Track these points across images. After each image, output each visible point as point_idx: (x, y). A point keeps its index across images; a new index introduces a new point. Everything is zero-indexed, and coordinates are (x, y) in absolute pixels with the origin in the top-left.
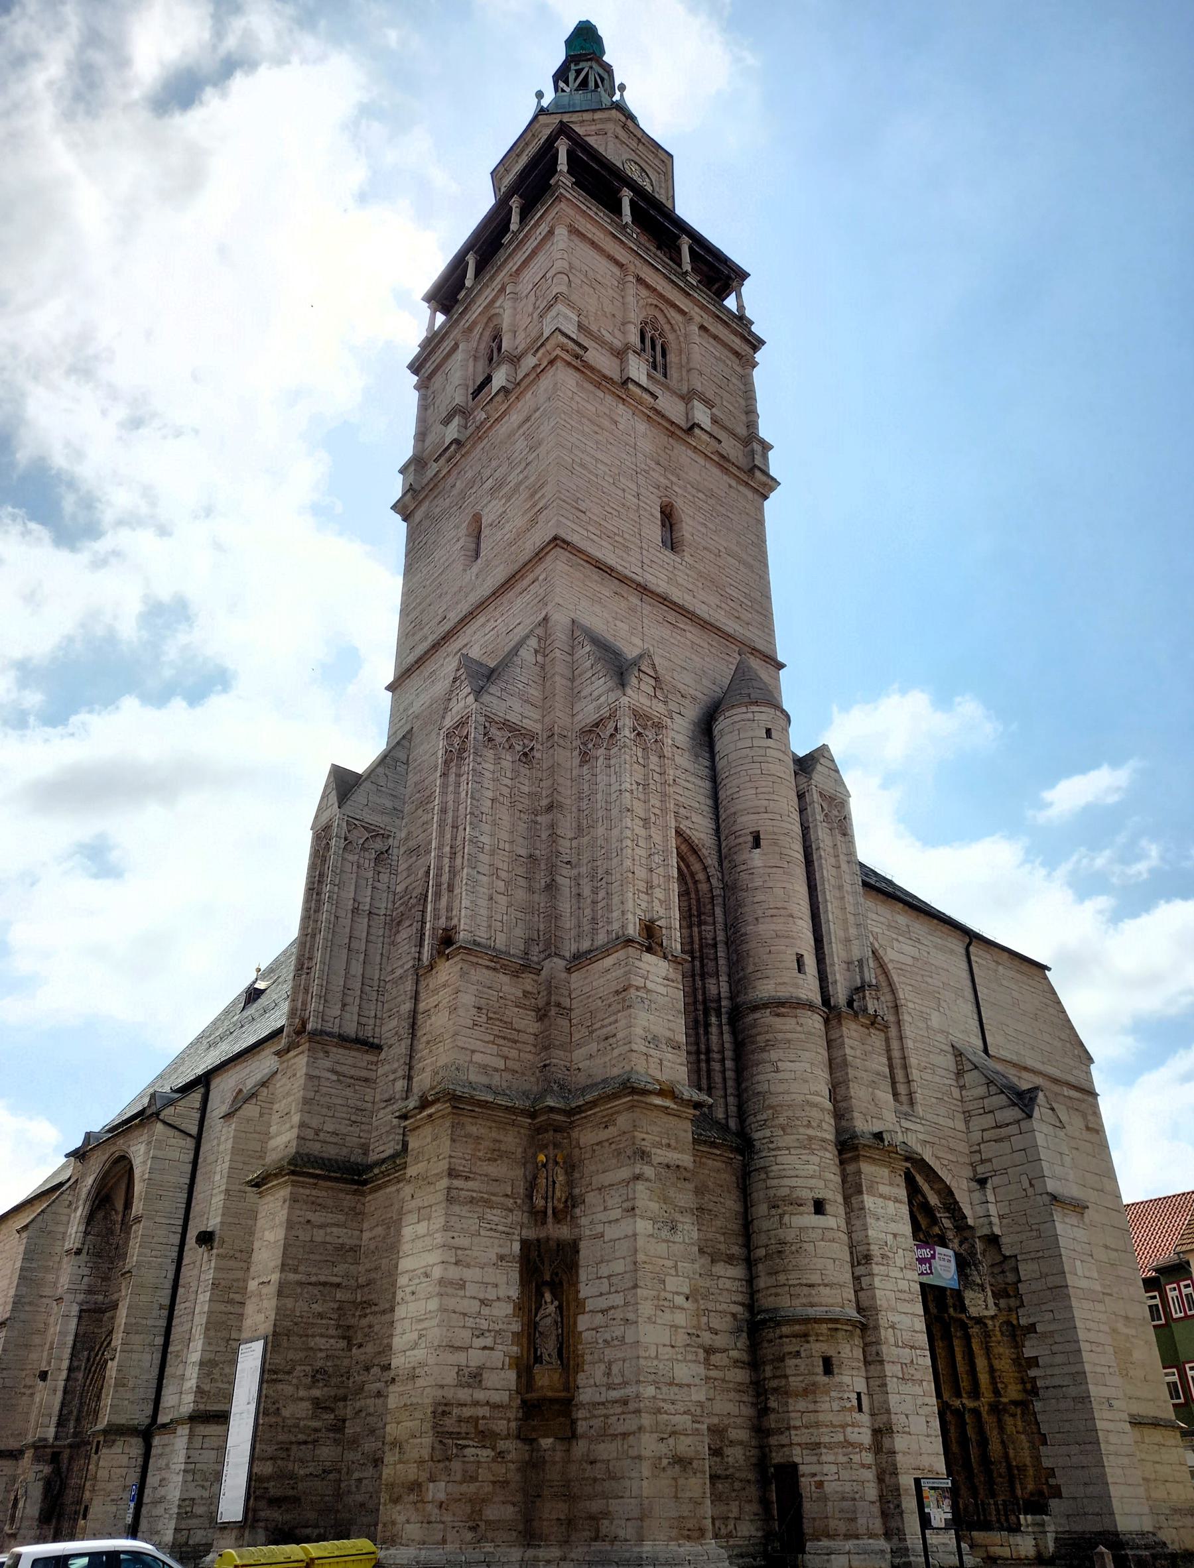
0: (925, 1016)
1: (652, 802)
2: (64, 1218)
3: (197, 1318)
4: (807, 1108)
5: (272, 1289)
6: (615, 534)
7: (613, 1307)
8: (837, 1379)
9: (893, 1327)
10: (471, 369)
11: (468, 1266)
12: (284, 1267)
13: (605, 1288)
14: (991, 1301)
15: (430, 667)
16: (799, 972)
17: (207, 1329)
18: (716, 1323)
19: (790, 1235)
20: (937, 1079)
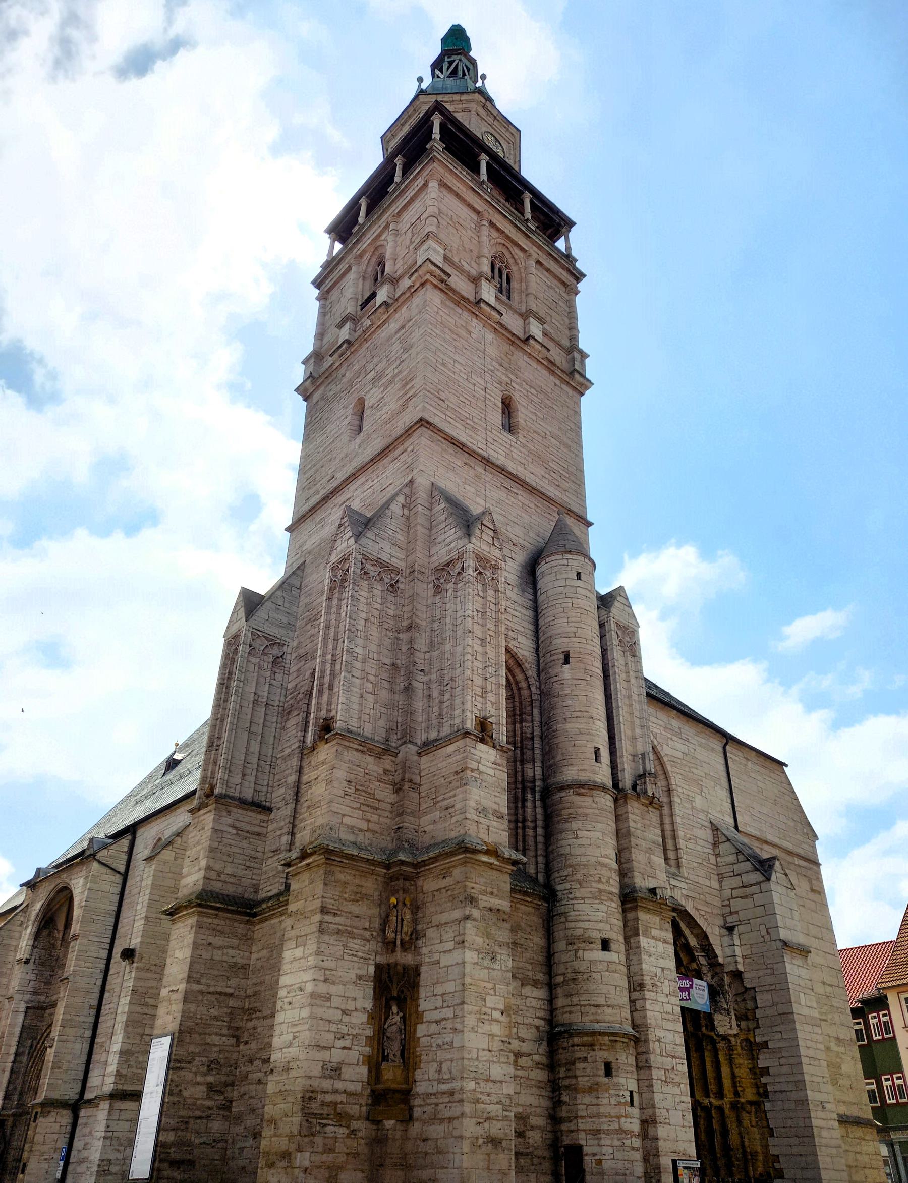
0: (691, 798)
1: (488, 626)
2: (17, 935)
3: (118, 1018)
4: (599, 867)
5: (179, 996)
6: (467, 418)
7: (445, 1019)
8: (615, 1080)
9: (659, 1041)
10: (360, 286)
11: (334, 983)
12: (189, 979)
13: (439, 1003)
14: (734, 1023)
15: (320, 515)
16: (596, 761)
17: (127, 1026)
18: (523, 1033)
19: (583, 966)
20: (699, 848)
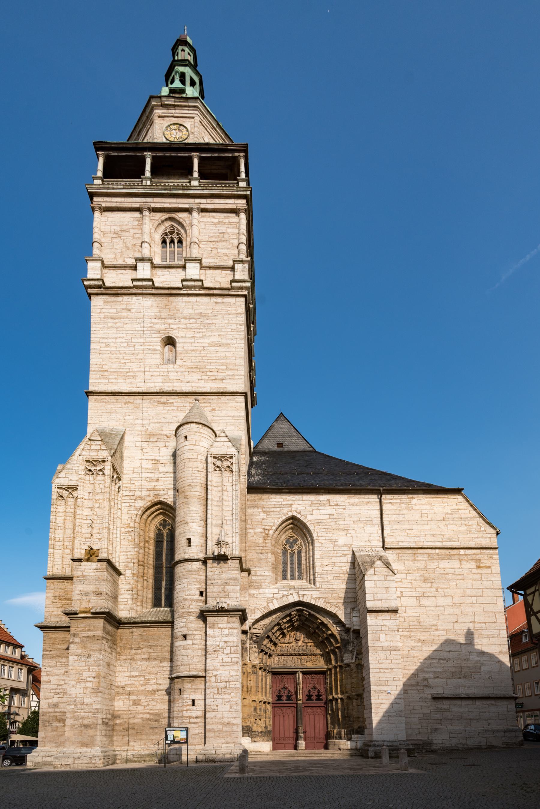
6: (127, 372)
